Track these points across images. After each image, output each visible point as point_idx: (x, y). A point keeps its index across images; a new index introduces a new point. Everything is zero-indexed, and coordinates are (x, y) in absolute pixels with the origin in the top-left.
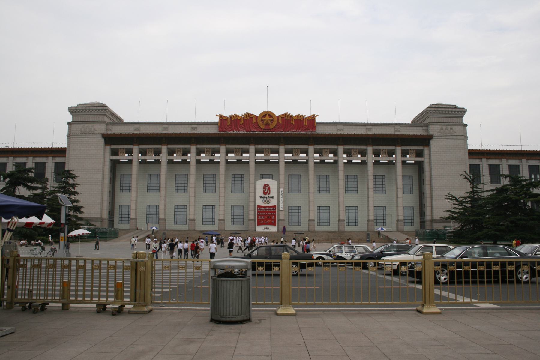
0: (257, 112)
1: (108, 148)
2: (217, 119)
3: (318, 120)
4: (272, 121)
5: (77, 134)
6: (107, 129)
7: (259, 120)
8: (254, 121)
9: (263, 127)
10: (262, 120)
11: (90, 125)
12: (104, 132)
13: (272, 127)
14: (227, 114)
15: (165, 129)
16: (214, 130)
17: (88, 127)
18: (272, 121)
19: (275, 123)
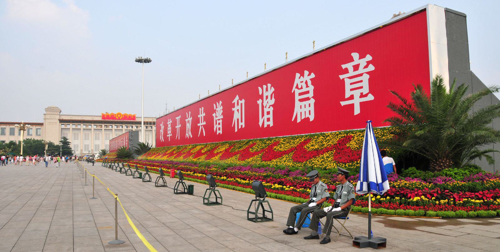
0: (115, 113)
1: (60, 124)
2: (101, 115)
3: (136, 116)
4: (121, 116)
5: (48, 119)
6: (60, 117)
7: (116, 115)
8: (114, 116)
9: (117, 118)
10: (117, 116)
11: (53, 116)
12: (59, 118)
13: (121, 118)
14: (105, 113)
15: (83, 118)
16: (100, 119)
17: (52, 116)
18: (121, 116)
19: (122, 116)
